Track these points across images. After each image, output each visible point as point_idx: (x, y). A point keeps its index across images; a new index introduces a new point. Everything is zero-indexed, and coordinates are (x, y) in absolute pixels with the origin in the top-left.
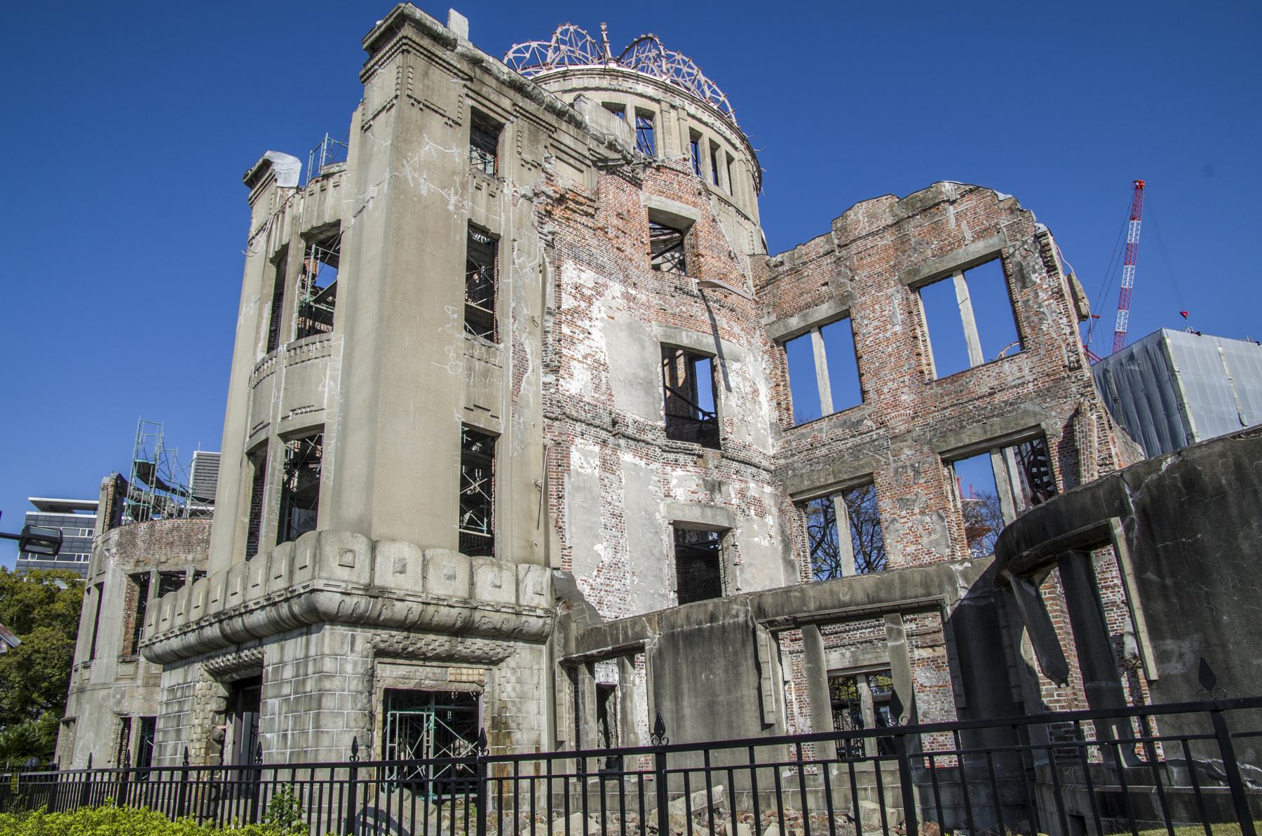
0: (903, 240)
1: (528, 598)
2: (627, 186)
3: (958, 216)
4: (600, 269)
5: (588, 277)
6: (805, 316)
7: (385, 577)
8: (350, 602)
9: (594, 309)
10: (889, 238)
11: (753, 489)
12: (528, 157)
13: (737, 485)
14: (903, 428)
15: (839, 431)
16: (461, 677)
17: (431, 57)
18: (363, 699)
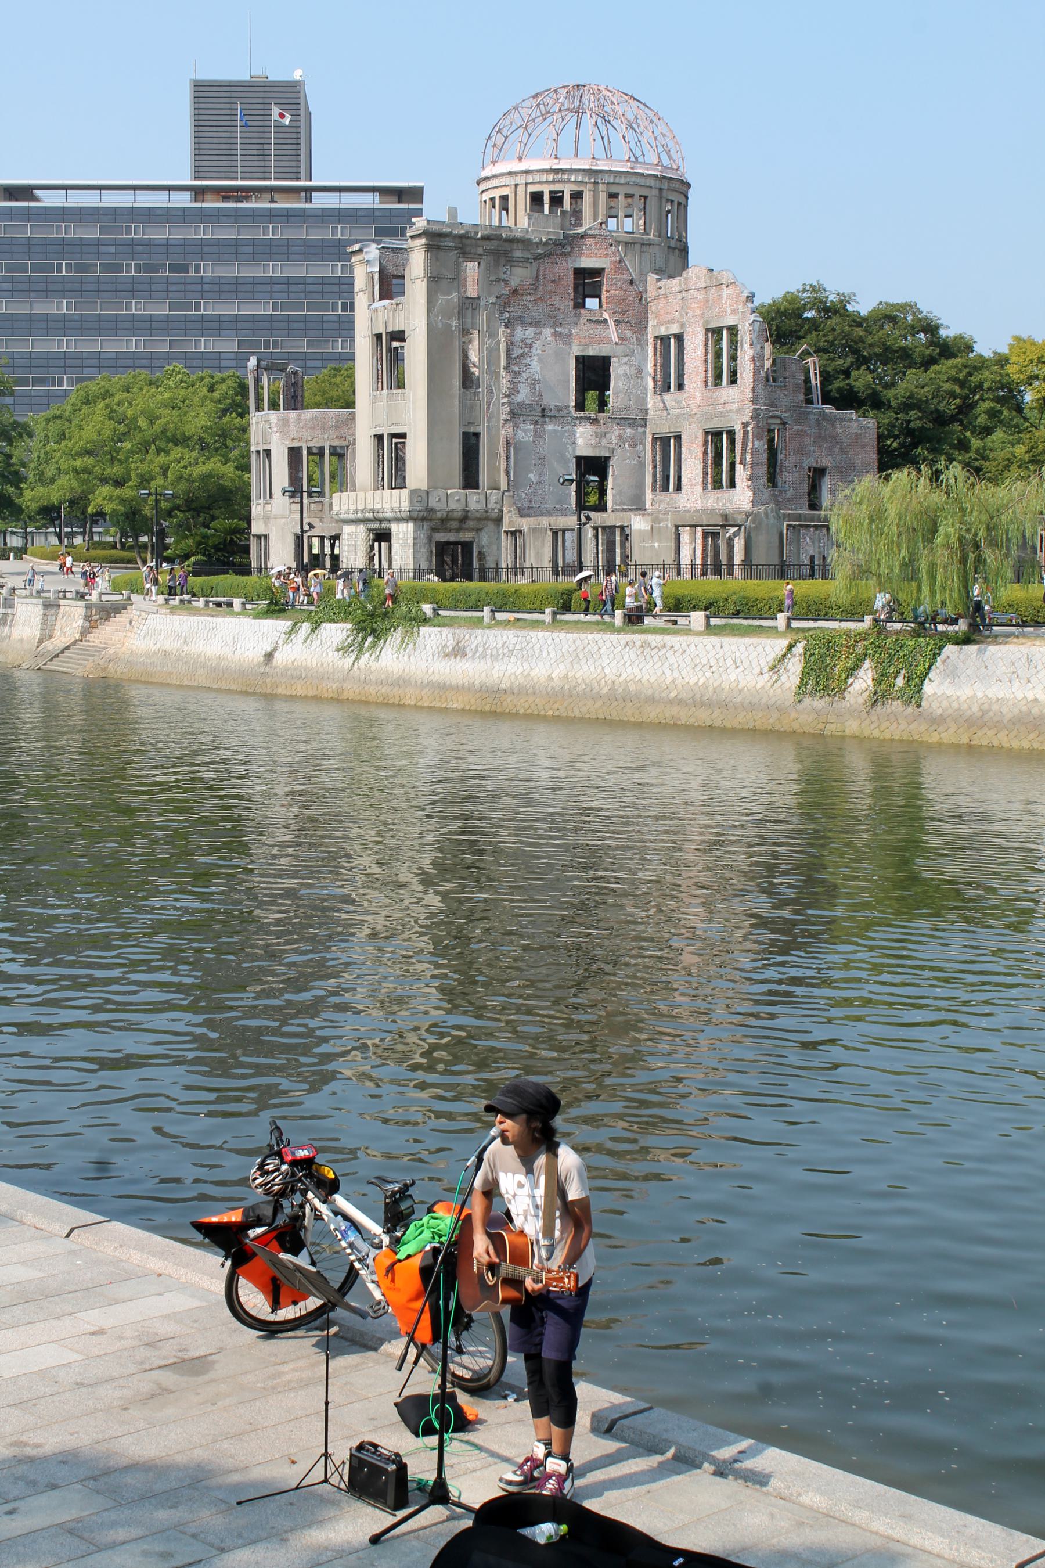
0: (707, 300)
1: (491, 505)
2: (559, 261)
3: (728, 296)
4: (538, 324)
5: (530, 331)
6: (667, 328)
7: (433, 503)
8: (421, 514)
9: (534, 351)
10: (701, 296)
11: (629, 431)
12: (493, 278)
13: (617, 432)
14: (695, 410)
15: (673, 403)
16: (466, 536)
17: (439, 248)
18: (427, 546)
